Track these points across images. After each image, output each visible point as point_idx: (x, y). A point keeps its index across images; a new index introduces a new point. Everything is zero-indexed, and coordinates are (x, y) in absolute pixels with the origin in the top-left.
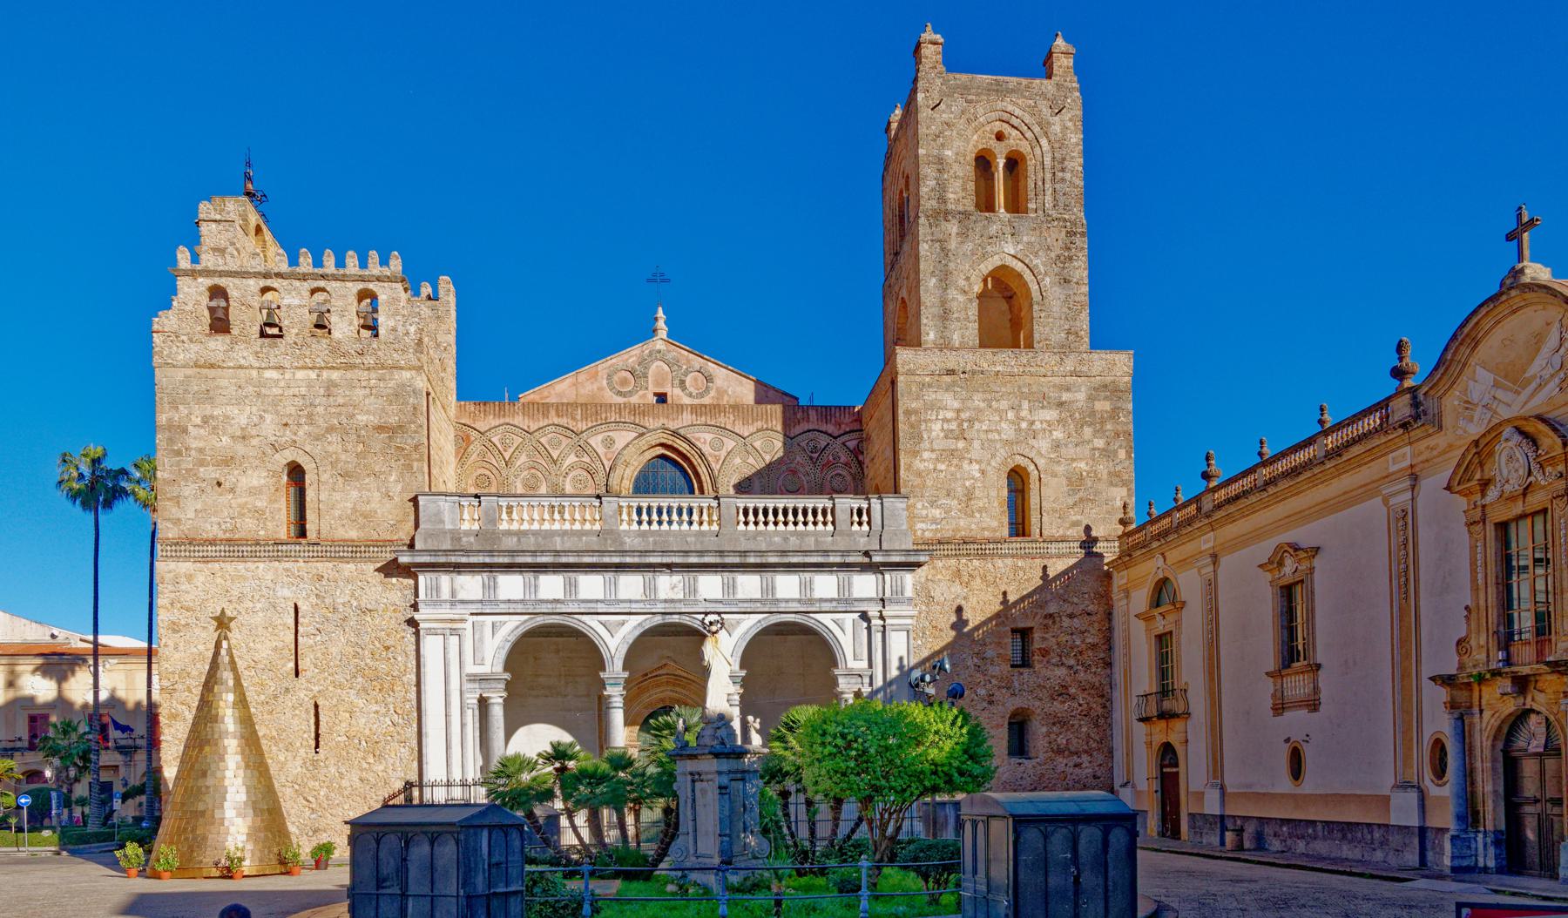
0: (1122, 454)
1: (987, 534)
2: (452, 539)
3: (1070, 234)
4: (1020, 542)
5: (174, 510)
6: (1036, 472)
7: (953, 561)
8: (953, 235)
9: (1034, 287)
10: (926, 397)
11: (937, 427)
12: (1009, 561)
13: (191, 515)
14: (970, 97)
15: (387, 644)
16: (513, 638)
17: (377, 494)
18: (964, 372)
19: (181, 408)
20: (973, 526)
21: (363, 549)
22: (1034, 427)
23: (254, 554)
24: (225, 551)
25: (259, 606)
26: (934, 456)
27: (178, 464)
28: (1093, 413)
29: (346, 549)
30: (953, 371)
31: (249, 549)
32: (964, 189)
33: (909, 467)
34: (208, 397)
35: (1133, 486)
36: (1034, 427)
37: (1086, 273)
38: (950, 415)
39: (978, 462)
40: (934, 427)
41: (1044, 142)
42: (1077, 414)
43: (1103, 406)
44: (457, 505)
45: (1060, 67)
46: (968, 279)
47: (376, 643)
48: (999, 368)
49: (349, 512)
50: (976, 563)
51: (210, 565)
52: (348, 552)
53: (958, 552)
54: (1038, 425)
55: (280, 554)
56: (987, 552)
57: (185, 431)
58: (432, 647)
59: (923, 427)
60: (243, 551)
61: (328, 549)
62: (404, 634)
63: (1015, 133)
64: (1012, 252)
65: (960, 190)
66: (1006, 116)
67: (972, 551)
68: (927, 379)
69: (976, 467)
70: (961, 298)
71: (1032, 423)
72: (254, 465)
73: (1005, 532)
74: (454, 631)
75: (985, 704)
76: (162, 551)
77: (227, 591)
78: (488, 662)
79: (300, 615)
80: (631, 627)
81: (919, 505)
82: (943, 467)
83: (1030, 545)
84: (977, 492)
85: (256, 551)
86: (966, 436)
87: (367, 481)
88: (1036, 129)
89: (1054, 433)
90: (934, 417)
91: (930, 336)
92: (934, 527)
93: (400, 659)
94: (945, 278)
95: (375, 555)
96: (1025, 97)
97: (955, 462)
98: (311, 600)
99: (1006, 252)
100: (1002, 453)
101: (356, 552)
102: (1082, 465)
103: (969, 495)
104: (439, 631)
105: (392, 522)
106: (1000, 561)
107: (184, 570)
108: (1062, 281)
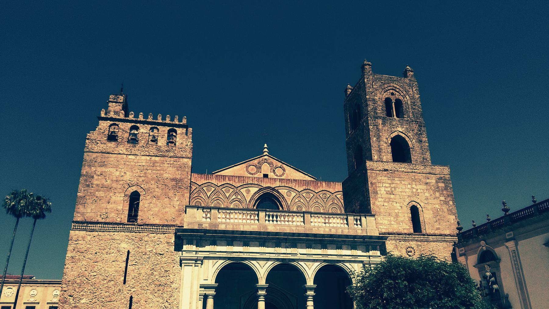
0: (451, 203)
1: (406, 231)
2: (199, 225)
3: (420, 126)
4: (418, 235)
5: (82, 209)
6: (421, 208)
7: (394, 242)
8: (381, 124)
9: (410, 143)
10: (378, 178)
11: (383, 189)
13: (89, 211)
14: (382, 81)
15: (167, 269)
16: (220, 268)
17: (169, 206)
18: (391, 170)
20: (400, 228)
22: (418, 191)
23: (114, 229)
25: (113, 251)
26: (383, 200)
27: (87, 190)
28: (438, 187)
30: (387, 169)
31: (112, 226)
32: (382, 110)
33: (374, 204)
34: (103, 165)
35: (457, 215)
36: (418, 191)
37: (427, 139)
38: (387, 185)
39: (399, 203)
41: (407, 97)
42: (433, 188)
43: (441, 185)
45: (410, 75)
46: (387, 139)
47: (162, 269)
48: (403, 170)
49: (157, 212)
50: (403, 243)
52: (154, 229)
54: (419, 191)
56: (407, 238)
59: (378, 189)
60: (109, 227)
61: (146, 227)
62: (174, 265)
63: (397, 93)
64: (401, 131)
65: (380, 110)
66: (394, 88)
68: (378, 172)
69: (398, 205)
70: (385, 145)
71: (417, 190)
72: (119, 192)
73: (412, 231)
76: (74, 226)
79: (130, 256)
80: (269, 265)
81: (379, 219)
82: (386, 204)
83: (422, 236)
85: (115, 227)
88: (405, 93)
89: (425, 193)
90: (382, 186)
91: (375, 157)
92: (385, 227)
94: (379, 138)
95: (166, 230)
96: (400, 83)
97: (390, 203)
99: (400, 130)
100: (408, 201)
101: (158, 229)
102: (437, 206)
103: (397, 215)
104: (190, 264)
105: (174, 217)
106: (412, 242)
107: (82, 235)
108: (419, 141)
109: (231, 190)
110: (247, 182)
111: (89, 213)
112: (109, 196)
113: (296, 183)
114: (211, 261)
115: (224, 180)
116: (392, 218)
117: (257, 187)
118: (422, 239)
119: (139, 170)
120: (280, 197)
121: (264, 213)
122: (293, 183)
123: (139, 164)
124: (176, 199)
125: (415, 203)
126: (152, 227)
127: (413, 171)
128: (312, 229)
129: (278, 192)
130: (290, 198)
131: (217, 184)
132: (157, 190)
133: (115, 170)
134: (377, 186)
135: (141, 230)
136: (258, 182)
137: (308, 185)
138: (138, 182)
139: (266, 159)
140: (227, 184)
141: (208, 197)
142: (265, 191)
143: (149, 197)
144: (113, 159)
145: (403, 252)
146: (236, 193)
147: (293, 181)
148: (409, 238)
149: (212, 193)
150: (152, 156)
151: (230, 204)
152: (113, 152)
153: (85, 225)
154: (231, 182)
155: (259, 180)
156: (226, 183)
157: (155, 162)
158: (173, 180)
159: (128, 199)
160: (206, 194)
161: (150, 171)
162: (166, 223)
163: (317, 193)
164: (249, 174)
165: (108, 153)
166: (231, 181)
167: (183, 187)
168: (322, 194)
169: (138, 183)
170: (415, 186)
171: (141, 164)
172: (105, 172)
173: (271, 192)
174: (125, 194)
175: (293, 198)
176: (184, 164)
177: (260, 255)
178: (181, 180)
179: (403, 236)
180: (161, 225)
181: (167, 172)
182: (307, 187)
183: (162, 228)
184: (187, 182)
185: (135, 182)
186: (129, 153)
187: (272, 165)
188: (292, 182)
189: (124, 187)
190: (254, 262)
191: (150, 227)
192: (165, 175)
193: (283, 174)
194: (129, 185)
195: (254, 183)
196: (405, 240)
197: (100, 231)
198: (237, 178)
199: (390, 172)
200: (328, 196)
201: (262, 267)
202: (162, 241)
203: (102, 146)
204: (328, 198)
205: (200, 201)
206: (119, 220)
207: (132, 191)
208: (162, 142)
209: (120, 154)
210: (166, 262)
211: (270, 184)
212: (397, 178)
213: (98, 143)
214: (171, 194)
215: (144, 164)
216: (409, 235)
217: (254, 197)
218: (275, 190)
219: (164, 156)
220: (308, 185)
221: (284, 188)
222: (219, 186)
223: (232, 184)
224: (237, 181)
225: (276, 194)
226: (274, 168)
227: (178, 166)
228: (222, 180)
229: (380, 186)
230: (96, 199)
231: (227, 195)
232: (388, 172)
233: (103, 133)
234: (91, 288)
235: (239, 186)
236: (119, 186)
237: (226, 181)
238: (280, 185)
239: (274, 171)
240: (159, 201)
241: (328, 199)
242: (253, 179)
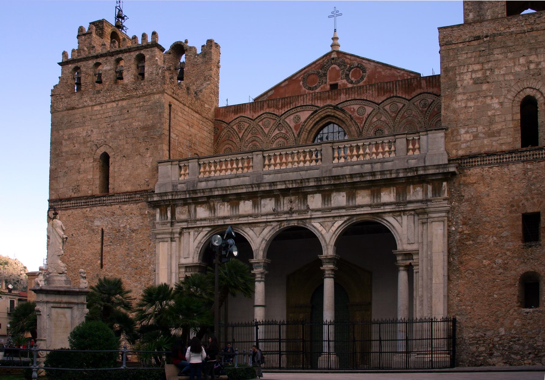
1: (504, 148)
2: (173, 186)
4: (530, 151)
12: (520, 165)
15: (143, 248)
17: (141, 165)
19: (60, 132)
21: (133, 196)
22: (540, 67)
24: (74, 203)
29: (125, 197)
36: (540, 67)
40: (465, 77)
44: (177, 166)
50: (496, 169)
51: (68, 211)
52: (126, 198)
53: (482, 163)
55: (97, 202)
56: (505, 160)
57: (61, 143)
58: (163, 249)
61: (118, 197)
62: (150, 242)
67: (493, 161)
73: (518, 145)
74: (172, 240)
75: (501, 270)
77: (75, 224)
78: (191, 256)
84: (497, 118)
86: (489, 80)
87: (136, 159)
93: (148, 256)
97: (480, 99)
98: (109, 226)
101: (130, 198)
104: (166, 240)
105: (147, 180)
106: (513, 166)
109: (272, 122)
110: (296, 105)
111: (62, 188)
112: (78, 164)
113: (373, 90)
114: (192, 232)
115: (262, 108)
116: (480, 128)
117: (310, 109)
118: (536, 158)
119: (105, 124)
120: (346, 119)
121: (260, 156)
122: (368, 91)
123: (105, 115)
124: (148, 155)
125: (532, 90)
126: (124, 197)
127: (535, 26)
128: (330, 170)
129: (342, 110)
130: (363, 118)
131: (253, 116)
132: (126, 147)
133: (82, 130)
134: (457, 73)
135: (113, 202)
136: (312, 101)
137: (395, 89)
138: (105, 140)
139: (333, 59)
140: (266, 113)
141: (240, 139)
142: (322, 114)
143: (118, 158)
144: (78, 116)
145: (494, 186)
146: (279, 126)
147: (368, 88)
148: (510, 159)
149: (244, 132)
150: (119, 100)
151: (272, 143)
152: (78, 107)
153: (60, 203)
154: (271, 110)
155: (313, 98)
156: (264, 112)
157: (123, 108)
158: (144, 128)
159: (97, 165)
160: (238, 135)
161: (117, 123)
162: (139, 189)
163: (409, 100)
164: (308, 89)
165: (73, 108)
166: (271, 107)
167: (156, 137)
168: (419, 101)
169: (106, 142)
170: (535, 56)
171: (106, 115)
172: (72, 134)
173: (333, 114)
174: (94, 159)
175: (368, 117)
176: (155, 103)
177: (253, 219)
178: (153, 127)
179: (498, 157)
180: (133, 192)
181: (137, 119)
182: (393, 94)
183: (135, 196)
184: (160, 128)
185: (102, 141)
186: (94, 104)
187: (343, 67)
188: (366, 90)
189: (92, 150)
190: (247, 230)
191: (122, 197)
192: (134, 124)
193: (362, 78)
194: (97, 147)
195: (305, 104)
196: (500, 164)
197: (73, 209)
198: (281, 101)
199: (485, 39)
200: (430, 101)
201: (258, 234)
202: (135, 213)
203: (66, 100)
204: (431, 104)
205: (230, 146)
206: (90, 192)
207: (101, 153)
208: (128, 77)
209: (84, 107)
210: (141, 239)
211: (330, 100)
212: (499, 50)
213: (62, 99)
214: (142, 150)
215: (110, 114)
216: (510, 152)
217: (306, 127)
218: (338, 108)
219: (130, 97)
220: (395, 89)
221: (352, 102)
222: (254, 120)
223: (273, 112)
224: (280, 106)
225: (341, 114)
226: (347, 70)
227: (148, 107)
228: (259, 109)
229: (462, 71)
230: (66, 170)
231: (266, 131)
232: (481, 41)
233: (66, 83)
234: (72, 274)
235: (283, 112)
236: (88, 150)
237: (264, 109)
238: (348, 99)
239: (347, 75)
240: (129, 160)
241: (429, 107)
242: (304, 98)
